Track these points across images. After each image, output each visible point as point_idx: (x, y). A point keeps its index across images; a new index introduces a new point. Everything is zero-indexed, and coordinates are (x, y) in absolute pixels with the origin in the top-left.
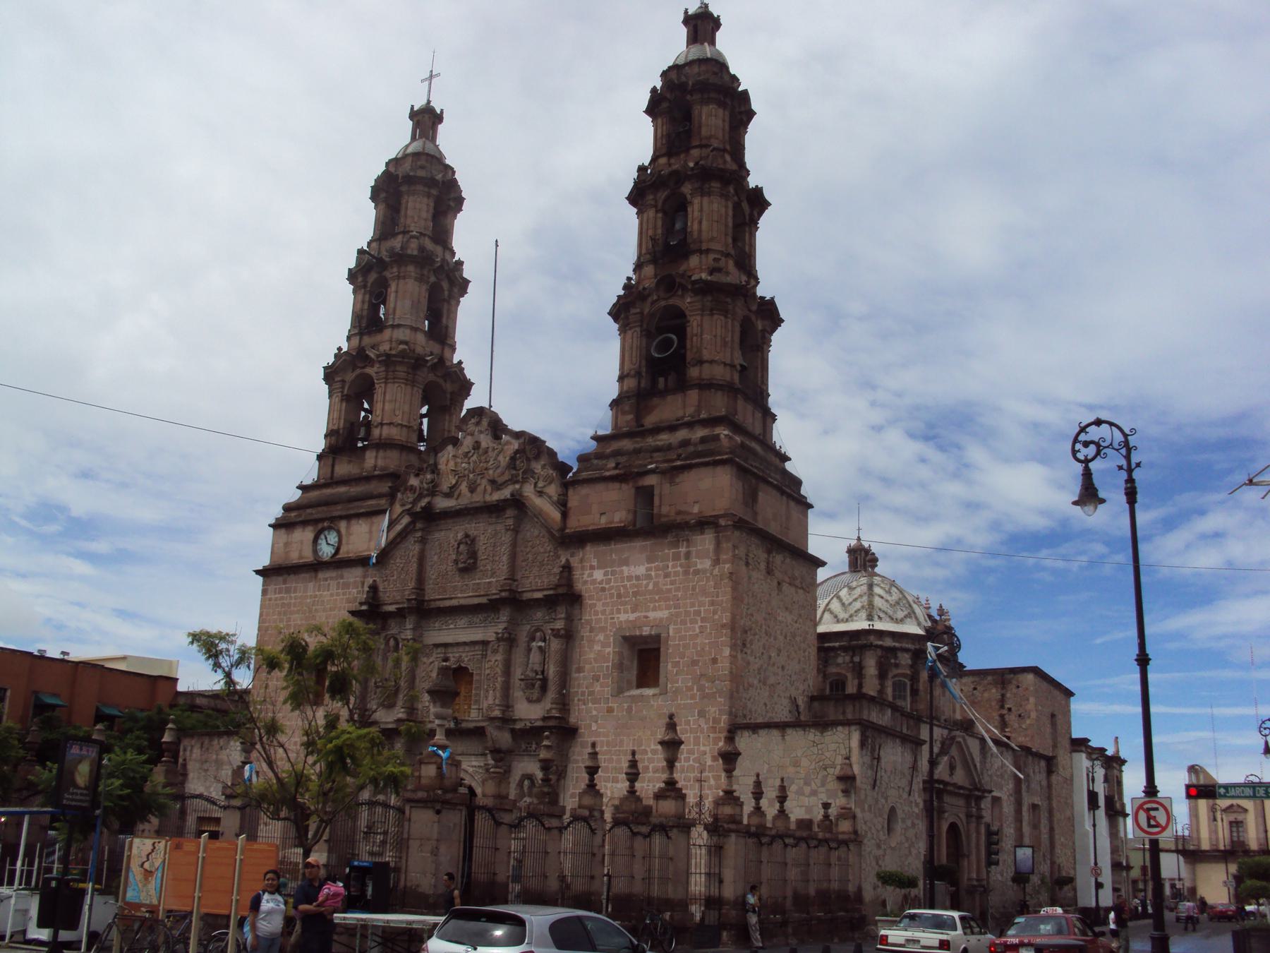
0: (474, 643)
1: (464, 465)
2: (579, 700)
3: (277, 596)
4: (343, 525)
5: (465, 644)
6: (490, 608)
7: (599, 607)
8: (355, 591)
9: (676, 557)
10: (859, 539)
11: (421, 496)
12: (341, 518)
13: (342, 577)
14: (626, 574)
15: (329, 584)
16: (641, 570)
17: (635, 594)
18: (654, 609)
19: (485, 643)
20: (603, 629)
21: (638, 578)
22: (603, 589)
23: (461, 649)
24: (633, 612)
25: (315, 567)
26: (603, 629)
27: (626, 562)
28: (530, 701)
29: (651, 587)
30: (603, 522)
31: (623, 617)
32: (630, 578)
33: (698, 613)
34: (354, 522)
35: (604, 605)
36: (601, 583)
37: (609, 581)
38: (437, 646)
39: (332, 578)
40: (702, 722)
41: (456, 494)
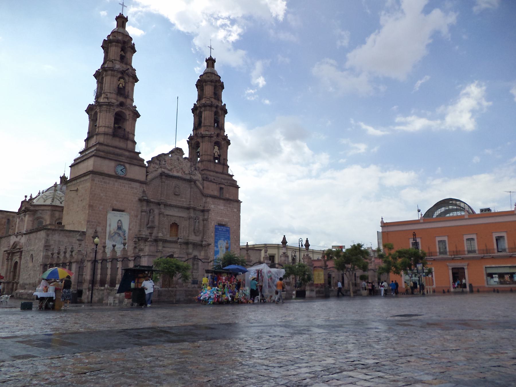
0: (180, 217)
1: (175, 163)
2: (208, 237)
3: (99, 183)
4: (127, 166)
5: (177, 217)
6: (188, 209)
7: (213, 214)
8: (136, 190)
9: (230, 207)
10: (64, 174)
11: (161, 167)
12: (127, 163)
13: (130, 185)
14: (219, 208)
15: (125, 186)
16: (222, 208)
17: (221, 213)
18: (225, 218)
19: (183, 217)
20: (214, 220)
21: (222, 210)
22: (214, 210)
23: (175, 217)
24: (221, 217)
25: (117, 177)
26: (214, 220)
27: (219, 205)
28: (196, 236)
29: (224, 212)
30: (212, 193)
31: (218, 218)
32: (220, 209)
33: (234, 221)
34: (132, 166)
35: (214, 214)
36: (213, 208)
37: (215, 209)
38: (167, 215)
39: (126, 184)
40: (235, 246)
41: (172, 171)
